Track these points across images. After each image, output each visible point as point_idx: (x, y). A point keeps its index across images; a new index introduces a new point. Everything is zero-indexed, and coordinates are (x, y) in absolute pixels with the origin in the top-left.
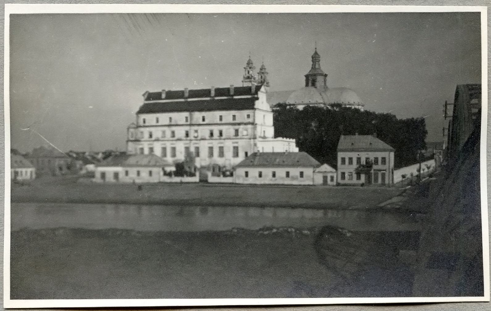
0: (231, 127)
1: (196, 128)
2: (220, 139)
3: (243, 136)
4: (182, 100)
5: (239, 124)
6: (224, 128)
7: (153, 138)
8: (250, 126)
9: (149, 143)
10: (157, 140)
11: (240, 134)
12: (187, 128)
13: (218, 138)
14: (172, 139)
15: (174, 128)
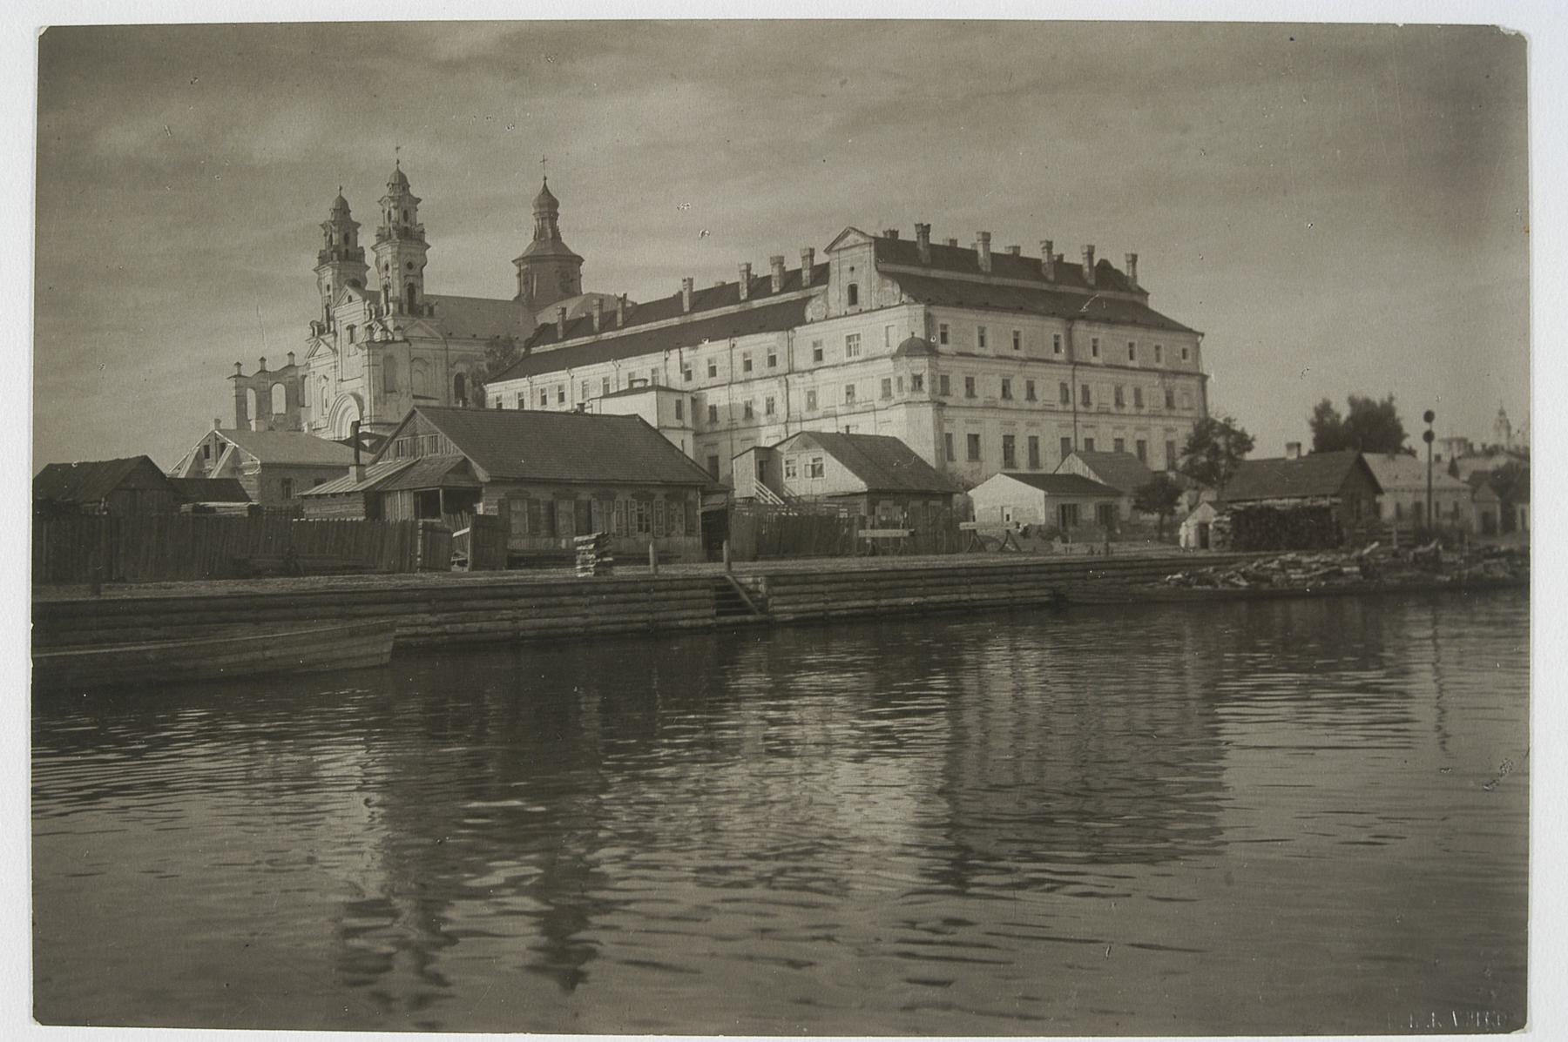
0: (1156, 380)
1: (1083, 375)
2: (1139, 415)
3: (1184, 409)
4: (981, 279)
5: (1176, 374)
6: (1144, 380)
7: (980, 401)
8: (1194, 383)
9: (968, 414)
10: (990, 406)
11: (1176, 404)
12: (1065, 373)
13: (1134, 411)
14: (1027, 405)
15: (1033, 370)
